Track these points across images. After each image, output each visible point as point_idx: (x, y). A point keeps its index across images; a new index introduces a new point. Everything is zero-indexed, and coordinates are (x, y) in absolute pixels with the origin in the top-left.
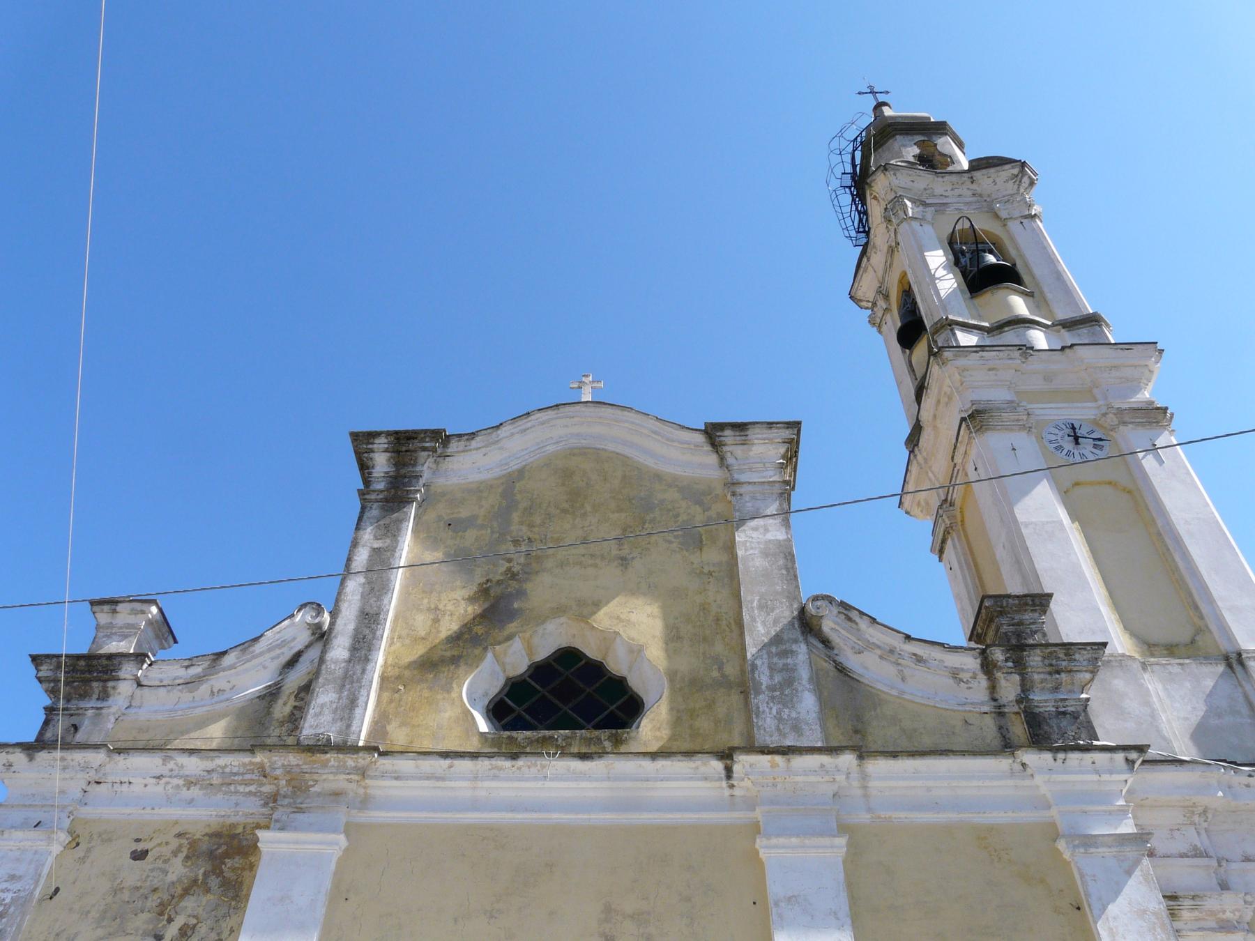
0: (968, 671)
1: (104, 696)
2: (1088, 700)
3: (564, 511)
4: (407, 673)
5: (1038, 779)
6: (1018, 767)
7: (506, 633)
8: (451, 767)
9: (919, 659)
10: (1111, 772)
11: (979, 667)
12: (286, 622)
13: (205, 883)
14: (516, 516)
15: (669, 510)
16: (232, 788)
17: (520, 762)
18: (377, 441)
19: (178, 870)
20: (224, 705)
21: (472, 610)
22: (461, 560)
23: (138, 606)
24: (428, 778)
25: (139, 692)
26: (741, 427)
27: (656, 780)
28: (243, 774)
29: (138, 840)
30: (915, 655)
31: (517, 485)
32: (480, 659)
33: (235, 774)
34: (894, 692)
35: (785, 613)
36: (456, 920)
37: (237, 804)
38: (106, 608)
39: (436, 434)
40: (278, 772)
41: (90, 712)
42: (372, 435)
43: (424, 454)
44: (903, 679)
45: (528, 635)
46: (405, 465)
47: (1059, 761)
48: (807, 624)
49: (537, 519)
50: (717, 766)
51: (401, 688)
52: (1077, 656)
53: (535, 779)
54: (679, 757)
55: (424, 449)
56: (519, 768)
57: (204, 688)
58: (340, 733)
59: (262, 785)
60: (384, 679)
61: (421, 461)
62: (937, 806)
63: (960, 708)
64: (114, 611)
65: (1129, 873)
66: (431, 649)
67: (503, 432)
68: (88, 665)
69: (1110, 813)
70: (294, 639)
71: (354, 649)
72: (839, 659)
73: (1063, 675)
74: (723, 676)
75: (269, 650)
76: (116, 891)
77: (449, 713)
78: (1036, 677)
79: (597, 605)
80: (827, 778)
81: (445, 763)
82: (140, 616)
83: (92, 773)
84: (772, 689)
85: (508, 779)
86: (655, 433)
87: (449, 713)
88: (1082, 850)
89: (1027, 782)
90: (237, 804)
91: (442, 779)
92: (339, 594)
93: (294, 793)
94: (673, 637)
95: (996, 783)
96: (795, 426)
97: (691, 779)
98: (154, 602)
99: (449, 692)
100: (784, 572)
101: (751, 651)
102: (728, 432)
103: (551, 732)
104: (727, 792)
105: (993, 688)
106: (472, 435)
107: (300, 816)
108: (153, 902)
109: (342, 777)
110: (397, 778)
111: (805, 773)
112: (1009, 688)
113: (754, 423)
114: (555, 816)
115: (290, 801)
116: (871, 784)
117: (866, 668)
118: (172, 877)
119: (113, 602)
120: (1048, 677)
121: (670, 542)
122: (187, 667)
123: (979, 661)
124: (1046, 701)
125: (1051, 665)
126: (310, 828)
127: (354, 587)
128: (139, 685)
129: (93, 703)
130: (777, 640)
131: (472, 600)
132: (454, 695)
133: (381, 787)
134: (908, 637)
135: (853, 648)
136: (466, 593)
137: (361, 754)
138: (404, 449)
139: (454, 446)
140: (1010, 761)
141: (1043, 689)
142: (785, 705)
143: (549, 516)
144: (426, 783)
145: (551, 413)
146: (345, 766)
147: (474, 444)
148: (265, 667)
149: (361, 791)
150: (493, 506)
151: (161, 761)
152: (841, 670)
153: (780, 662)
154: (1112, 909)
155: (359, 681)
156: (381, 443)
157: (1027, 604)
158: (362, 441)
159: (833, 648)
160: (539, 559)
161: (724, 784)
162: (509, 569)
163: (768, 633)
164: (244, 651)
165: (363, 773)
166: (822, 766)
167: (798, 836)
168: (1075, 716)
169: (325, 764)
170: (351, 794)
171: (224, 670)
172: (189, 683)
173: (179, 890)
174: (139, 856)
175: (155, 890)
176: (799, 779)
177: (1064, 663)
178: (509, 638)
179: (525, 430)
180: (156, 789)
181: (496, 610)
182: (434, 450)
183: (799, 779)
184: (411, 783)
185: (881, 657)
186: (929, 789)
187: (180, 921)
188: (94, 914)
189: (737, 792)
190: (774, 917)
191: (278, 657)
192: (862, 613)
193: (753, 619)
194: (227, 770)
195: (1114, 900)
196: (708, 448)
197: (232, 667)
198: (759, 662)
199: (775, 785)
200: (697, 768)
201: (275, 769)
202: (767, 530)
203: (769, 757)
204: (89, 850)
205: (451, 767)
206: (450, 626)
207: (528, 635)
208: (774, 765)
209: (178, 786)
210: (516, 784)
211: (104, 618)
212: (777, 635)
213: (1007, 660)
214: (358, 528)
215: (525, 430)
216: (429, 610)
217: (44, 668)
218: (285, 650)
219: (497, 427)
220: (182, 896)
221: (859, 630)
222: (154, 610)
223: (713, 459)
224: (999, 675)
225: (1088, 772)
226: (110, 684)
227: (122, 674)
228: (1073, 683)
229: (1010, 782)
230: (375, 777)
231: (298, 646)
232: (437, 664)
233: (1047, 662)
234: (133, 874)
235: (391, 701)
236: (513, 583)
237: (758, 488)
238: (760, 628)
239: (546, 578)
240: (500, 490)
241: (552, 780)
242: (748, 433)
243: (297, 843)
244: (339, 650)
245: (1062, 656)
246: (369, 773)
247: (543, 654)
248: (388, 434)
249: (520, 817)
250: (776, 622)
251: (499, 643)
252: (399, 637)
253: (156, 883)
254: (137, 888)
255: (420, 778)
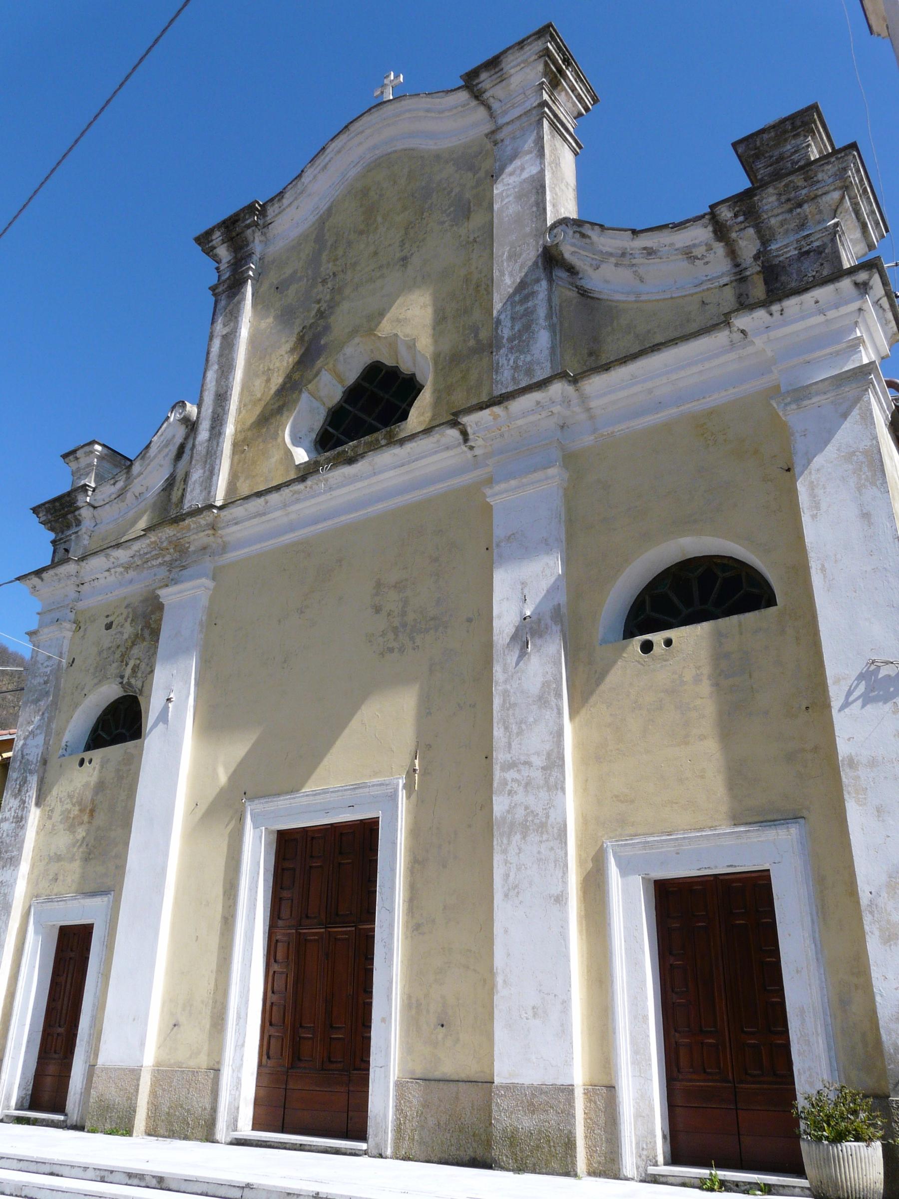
0: (700, 245)
1: (78, 523)
2: (837, 225)
3: (361, 233)
4: (249, 434)
5: (759, 342)
6: (737, 336)
7: (315, 371)
8: (267, 503)
9: (650, 252)
10: (837, 307)
11: (711, 235)
12: (165, 425)
13: (142, 635)
14: (324, 257)
15: (444, 189)
16: (149, 563)
17: (309, 482)
18: (214, 237)
19: (128, 630)
20: (143, 504)
21: (291, 359)
22: (286, 316)
23: (87, 449)
24: (255, 517)
25: (96, 512)
26: (493, 63)
27: (409, 463)
28: (150, 552)
29: (107, 616)
30: (645, 249)
31: (327, 224)
32: (296, 401)
33: (147, 553)
34: (632, 298)
35: (531, 253)
36: (279, 621)
37: (155, 575)
38: (71, 457)
39: (250, 209)
40: (165, 544)
41: (73, 537)
42: (209, 233)
43: (249, 231)
44: (642, 280)
45: (331, 366)
46: (241, 248)
47: (777, 315)
48: (551, 260)
49: (340, 252)
50: (453, 434)
51: (246, 448)
52: (820, 176)
53: (325, 492)
54: (421, 436)
55: (248, 227)
56: (311, 487)
57: (129, 495)
58: (204, 500)
59: (164, 556)
60: (235, 445)
61: (250, 238)
62: (660, 405)
63: (698, 289)
64: (77, 459)
65: (845, 416)
66: (265, 406)
67: (306, 179)
68: (61, 505)
69: (838, 353)
70: (174, 436)
71: (212, 428)
72: (583, 283)
73: (806, 206)
74: (478, 341)
75: (160, 452)
76: (100, 653)
77: (276, 456)
78: (773, 221)
79: (382, 314)
80: (544, 414)
81: (261, 500)
82: (92, 455)
83: (74, 579)
84: (511, 340)
85: (305, 499)
86: (428, 111)
87: (276, 456)
88: (794, 406)
89: (750, 350)
90: (155, 575)
91: (264, 514)
92: (203, 386)
93: (181, 556)
94: (440, 319)
96: (546, 31)
97: (436, 452)
98: (94, 442)
99: (276, 439)
100: (534, 209)
101: (497, 306)
102: (484, 76)
103: (340, 449)
104: (469, 454)
105: (732, 253)
106: (281, 195)
107: (185, 572)
108: (118, 655)
109: (202, 534)
110: (236, 524)
111: (524, 415)
112: (748, 244)
113: (504, 52)
114: (343, 518)
115: (179, 562)
116: (593, 404)
117: (607, 282)
118: (126, 636)
119: (74, 452)
120: (788, 216)
121: (443, 223)
122: (114, 484)
123: (710, 228)
124: (786, 246)
125: (789, 200)
126: (191, 578)
127: (211, 375)
128: (95, 508)
129: (74, 530)
130: (522, 286)
131: (292, 351)
132: (279, 440)
133: (232, 533)
134: (635, 232)
135: (591, 265)
136: (288, 347)
137: (205, 513)
138: (234, 234)
139: (271, 211)
140: (727, 332)
141: (787, 232)
142: (521, 352)
143: (349, 244)
144: (255, 521)
145: (343, 138)
146: (201, 526)
147: (285, 202)
148: (161, 466)
149: (220, 540)
150: (308, 255)
151: (105, 559)
152: (584, 293)
153: (520, 309)
154: (818, 461)
155: (215, 452)
156: (217, 236)
157: (785, 132)
158: (204, 240)
159: (577, 273)
160: (340, 290)
161: (465, 449)
162: (319, 310)
163: (513, 283)
164: (143, 458)
165: (213, 527)
166: (538, 403)
167: (515, 478)
168: (819, 251)
169: (189, 528)
170: (214, 545)
171: (135, 478)
172: (121, 495)
173: (130, 644)
174: (109, 626)
175: (118, 647)
176: (520, 422)
177: (804, 192)
178: (317, 374)
179: (325, 167)
180: (111, 579)
181: (310, 351)
182: (256, 224)
183: (520, 422)
184: (247, 524)
185: (617, 265)
186: (650, 391)
187: (131, 663)
188: (92, 670)
189: (477, 452)
190: (495, 557)
191: (167, 455)
192: (593, 224)
193: (502, 274)
194: (142, 552)
195: (821, 450)
196: (474, 103)
197: (140, 474)
198: (502, 317)
199: (502, 436)
200: (438, 441)
201: (162, 543)
202: (523, 169)
203: (487, 412)
204: (85, 630)
205: (267, 503)
206: (277, 380)
207: (331, 366)
208: (496, 417)
209: (121, 573)
210: (313, 501)
211: (74, 465)
212: (522, 282)
213: (736, 216)
214: (213, 323)
215: (325, 167)
216: (263, 373)
217: (40, 515)
218: (170, 447)
219: (300, 176)
220: (131, 647)
221: (592, 244)
222: (98, 448)
223: (482, 112)
224: (734, 235)
225: (811, 315)
226: (77, 513)
227: (80, 504)
228: (820, 212)
229: (732, 356)
230: (223, 528)
231: (179, 440)
232: (267, 418)
233: (783, 198)
234: (107, 639)
235: (240, 461)
236: (321, 322)
237: (517, 124)
238: (506, 279)
239: (345, 306)
240: (314, 236)
241: (339, 487)
242: (503, 65)
243: (180, 592)
244: (203, 434)
245: (801, 183)
246: (220, 525)
247: (352, 375)
248: (218, 226)
249: (320, 526)
250: (521, 267)
251: (310, 382)
252: (245, 406)
253: (119, 642)
254: (110, 648)
255: (251, 518)
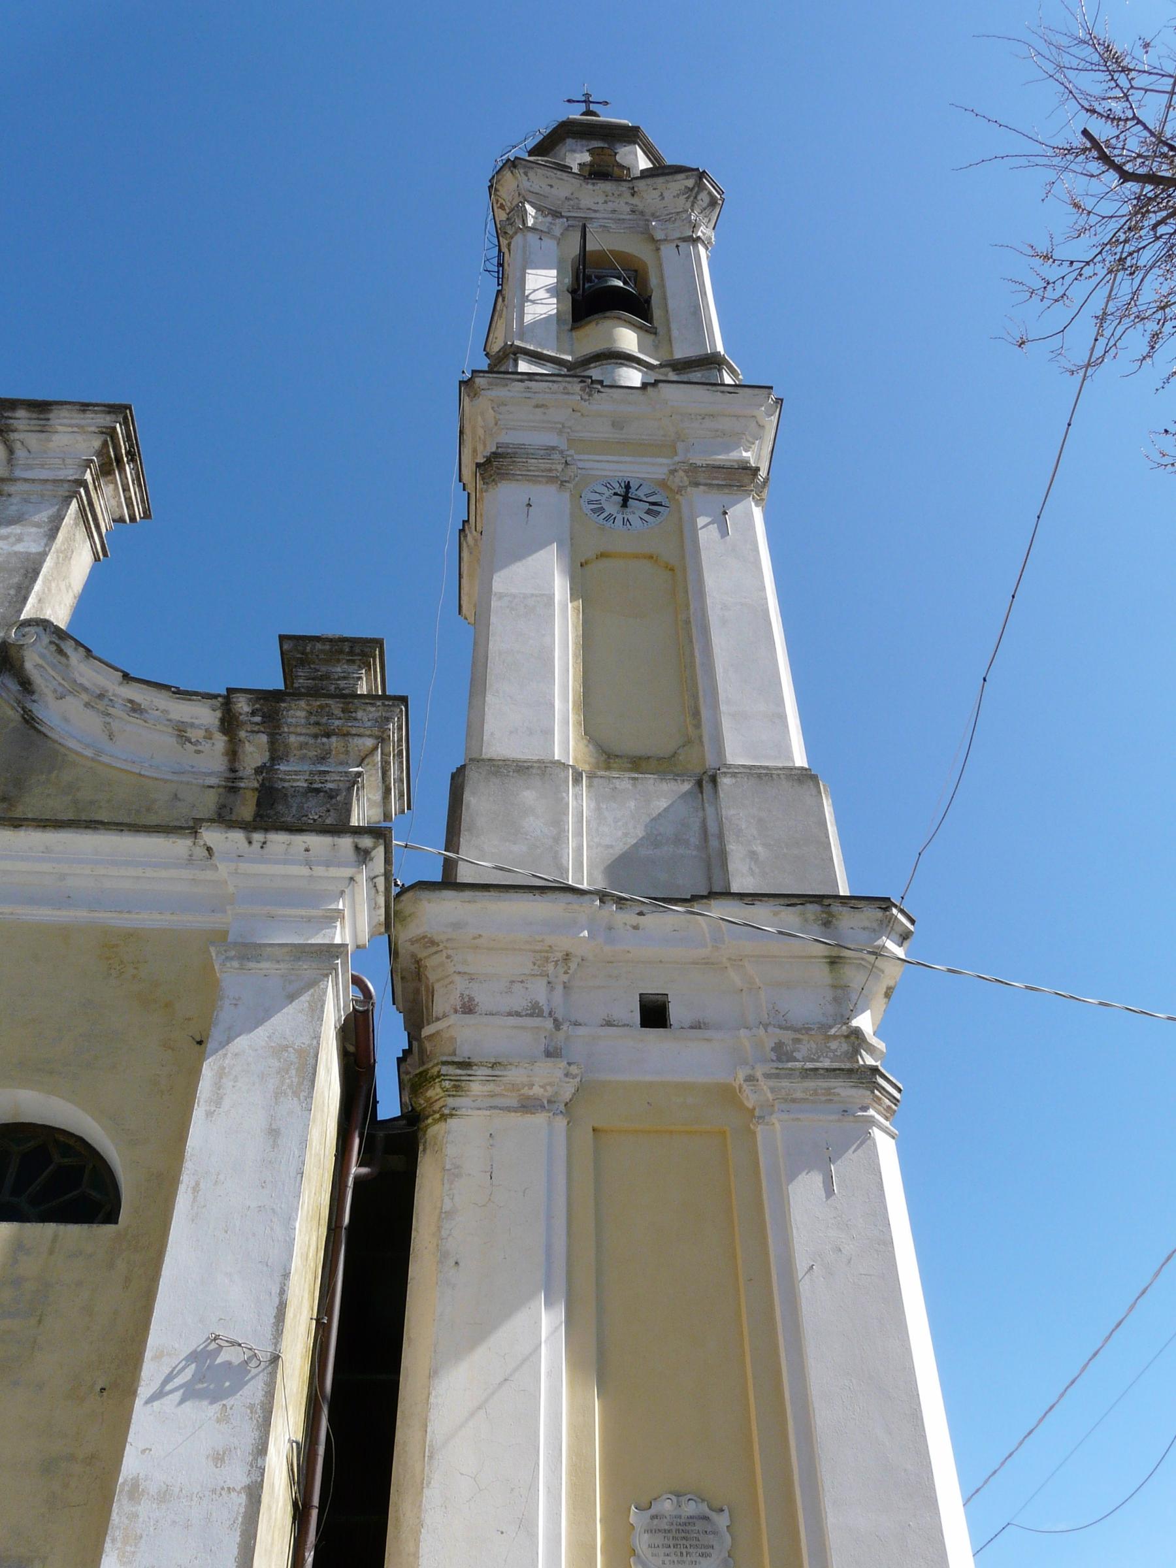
0: (199, 727)
2: (359, 774)
5: (224, 869)
6: (200, 852)
9: (135, 708)
10: (328, 864)
11: (217, 723)
26: (41, 408)
30: (131, 701)
34: (89, 753)
44: (111, 737)
47: (256, 846)
52: (360, 714)
62: (67, 900)
63: (175, 778)
65: (292, 998)
69: (309, 919)
73: (334, 739)
78: (292, 739)
88: (236, 964)
89: (209, 875)
95: (164, 874)
96: (120, 410)
100: (12, 592)
102: (21, 413)
105: (233, 754)
112: (255, 751)
117: (66, 720)
120: (311, 741)
123: (219, 714)
124: (296, 773)
125: (317, 724)
134: (126, 676)
135: (55, 691)
140: (189, 842)
152: (29, 720)
154: (242, 1043)
157: (341, 652)
159: (32, 693)
168: (331, 795)
177: (337, 723)
186: (63, 877)
192: (78, 643)
195: (251, 1030)
202: (19, 539)
213: (253, 713)
221: (67, 666)
224: (242, 734)
228: (347, 752)
229: (186, 873)
233: (313, 719)
237: (38, 487)
242: (51, 416)
